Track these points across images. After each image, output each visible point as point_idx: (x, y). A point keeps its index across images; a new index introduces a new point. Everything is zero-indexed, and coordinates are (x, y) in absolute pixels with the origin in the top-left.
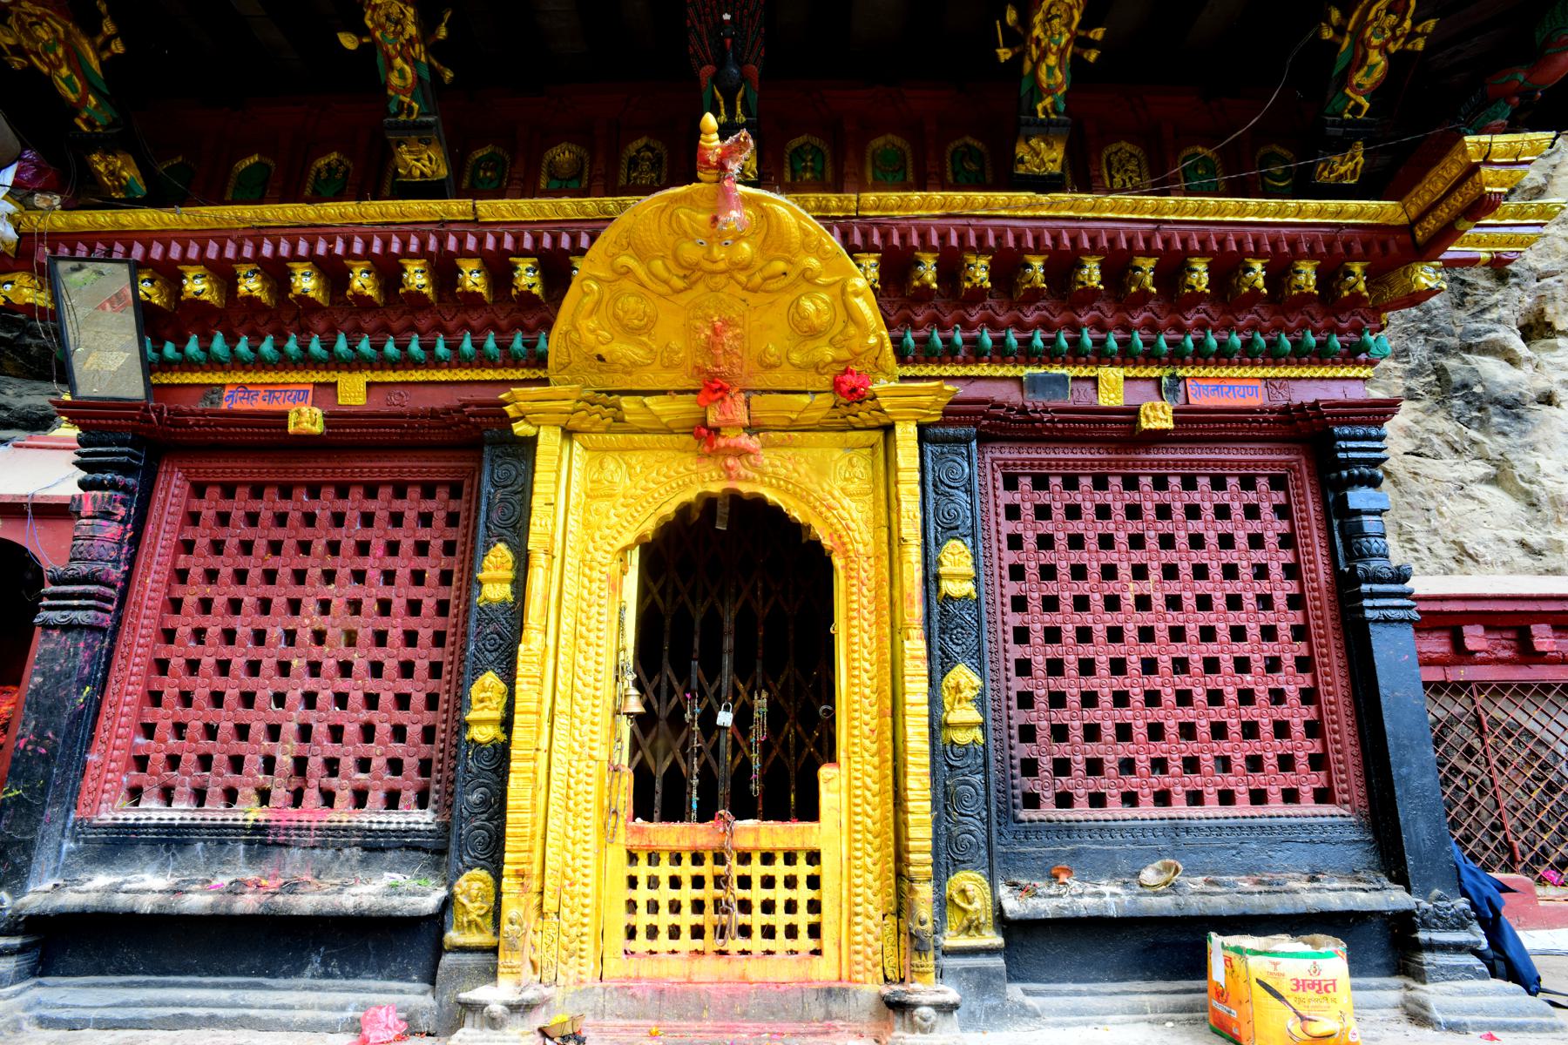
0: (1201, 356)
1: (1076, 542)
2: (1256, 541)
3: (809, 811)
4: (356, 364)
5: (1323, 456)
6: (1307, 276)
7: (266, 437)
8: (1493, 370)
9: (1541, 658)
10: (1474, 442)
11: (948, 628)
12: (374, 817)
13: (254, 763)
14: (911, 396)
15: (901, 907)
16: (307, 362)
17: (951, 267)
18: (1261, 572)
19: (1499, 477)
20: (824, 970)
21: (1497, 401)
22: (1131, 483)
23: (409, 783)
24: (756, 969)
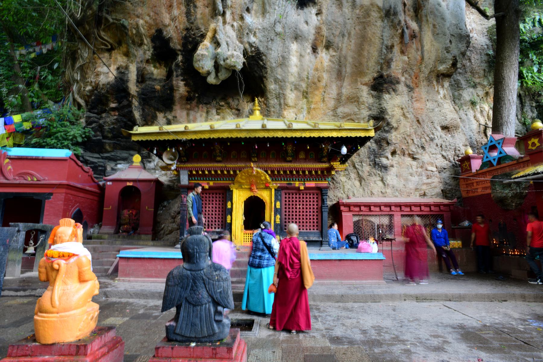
0: (307, 181)
4: (212, 180)
5: (321, 192)
6: (319, 172)
8: (384, 161)
9: (372, 211)
10: (379, 174)
11: (277, 211)
14: (274, 185)
16: (206, 180)
18: (314, 205)
19: (382, 180)
21: (383, 167)
22: (300, 194)
23: (220, 226)
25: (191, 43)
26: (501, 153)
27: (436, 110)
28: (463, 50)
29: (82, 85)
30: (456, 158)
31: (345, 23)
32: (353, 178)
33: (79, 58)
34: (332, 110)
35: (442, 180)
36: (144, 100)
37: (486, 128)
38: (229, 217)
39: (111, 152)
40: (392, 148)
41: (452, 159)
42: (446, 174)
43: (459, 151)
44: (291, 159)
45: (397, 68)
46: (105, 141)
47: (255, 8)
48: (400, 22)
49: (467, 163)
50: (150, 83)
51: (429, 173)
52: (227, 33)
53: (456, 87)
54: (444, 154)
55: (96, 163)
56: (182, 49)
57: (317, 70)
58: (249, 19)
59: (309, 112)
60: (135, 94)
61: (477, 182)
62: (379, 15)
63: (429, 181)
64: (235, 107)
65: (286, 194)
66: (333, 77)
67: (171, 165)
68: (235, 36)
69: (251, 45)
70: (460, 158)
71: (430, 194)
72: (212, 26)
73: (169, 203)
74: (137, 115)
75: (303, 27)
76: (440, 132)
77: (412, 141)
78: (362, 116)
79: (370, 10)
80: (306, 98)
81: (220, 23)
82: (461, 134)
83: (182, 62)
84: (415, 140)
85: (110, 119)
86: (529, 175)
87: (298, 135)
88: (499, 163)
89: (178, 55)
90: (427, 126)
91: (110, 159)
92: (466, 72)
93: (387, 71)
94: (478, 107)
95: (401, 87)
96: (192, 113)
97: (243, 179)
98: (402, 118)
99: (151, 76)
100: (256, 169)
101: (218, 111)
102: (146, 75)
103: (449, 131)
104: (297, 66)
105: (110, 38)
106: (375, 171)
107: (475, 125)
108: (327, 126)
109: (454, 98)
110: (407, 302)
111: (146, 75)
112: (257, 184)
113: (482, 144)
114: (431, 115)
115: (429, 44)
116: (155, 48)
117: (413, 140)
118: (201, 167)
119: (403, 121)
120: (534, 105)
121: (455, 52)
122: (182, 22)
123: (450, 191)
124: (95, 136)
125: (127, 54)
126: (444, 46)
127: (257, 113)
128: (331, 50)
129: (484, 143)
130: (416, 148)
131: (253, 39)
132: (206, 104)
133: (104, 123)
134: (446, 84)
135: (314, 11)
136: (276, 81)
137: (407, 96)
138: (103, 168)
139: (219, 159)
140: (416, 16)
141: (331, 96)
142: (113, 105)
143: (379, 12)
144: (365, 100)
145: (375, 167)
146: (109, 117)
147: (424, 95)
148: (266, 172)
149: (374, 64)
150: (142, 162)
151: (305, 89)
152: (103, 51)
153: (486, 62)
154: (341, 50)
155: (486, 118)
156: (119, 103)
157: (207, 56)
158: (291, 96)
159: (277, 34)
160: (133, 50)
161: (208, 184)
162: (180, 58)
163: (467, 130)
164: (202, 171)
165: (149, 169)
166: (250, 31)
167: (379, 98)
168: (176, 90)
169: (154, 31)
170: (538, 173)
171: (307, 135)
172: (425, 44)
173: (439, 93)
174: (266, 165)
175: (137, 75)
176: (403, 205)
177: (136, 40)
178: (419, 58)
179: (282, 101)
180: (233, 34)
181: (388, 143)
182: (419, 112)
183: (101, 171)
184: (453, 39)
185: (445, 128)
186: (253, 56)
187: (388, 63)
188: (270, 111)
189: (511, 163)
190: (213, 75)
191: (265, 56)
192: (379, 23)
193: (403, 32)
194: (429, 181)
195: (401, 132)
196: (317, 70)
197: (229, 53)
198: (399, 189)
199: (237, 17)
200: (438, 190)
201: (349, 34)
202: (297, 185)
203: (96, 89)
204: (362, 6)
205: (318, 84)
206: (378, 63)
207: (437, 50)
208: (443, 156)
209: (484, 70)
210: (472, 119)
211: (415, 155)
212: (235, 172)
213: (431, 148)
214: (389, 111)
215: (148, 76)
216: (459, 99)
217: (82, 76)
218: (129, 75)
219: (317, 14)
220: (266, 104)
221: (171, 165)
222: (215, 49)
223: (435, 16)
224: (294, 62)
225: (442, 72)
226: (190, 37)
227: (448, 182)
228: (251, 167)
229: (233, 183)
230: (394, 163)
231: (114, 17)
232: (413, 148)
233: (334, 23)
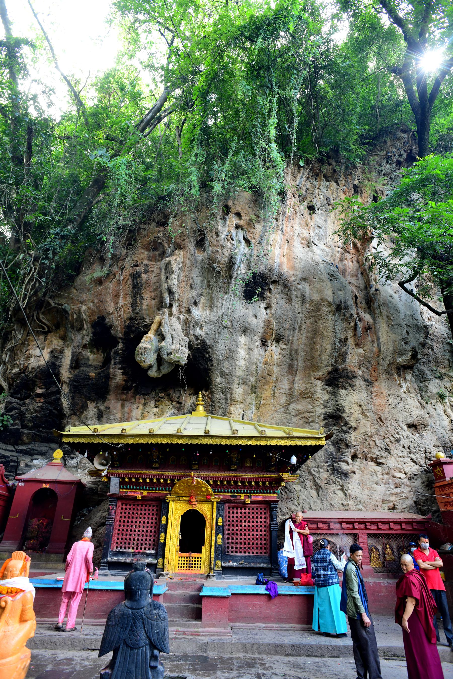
0: (254, 493)
1: (237, 517)
2: (261, 518)
3: (200, 552)
4: (146, 490)
6: (267, 484)
7: (134, 499)
8: (344, 466)
9: (332, 529)
11: (219, 529)
12: (147, 551)
13: (132, 544)
14: (216, 498)
15: (210, 564)
16: (140, 489)
17: (222, 482)
19: (342, 490)
20: (201, 572)
23: (151, 547)
24: (193, 572)
25: (135, 332)
27: (400, 405)
28: (422, 340)
29: (9, 367)
30: (428, 462)
31: (295, 317)
32: (309, 486)
33: (11, 339)
34: (283, 407)
35: (414, 489)
36: (75, 387)
38: (163, 535)
39: (28, 444)
40: (352, 451)
41: (423, 463)
42: (418, 483)
44: (235, 467)
45: (354, 357)
46: (23, 431)
47: (202, 301)
48: (352, 315)
49: (439, 469)
50: (85, 369)
51: (397, 480)
52: (173, 326)
53: (421, 378)
55: (9, 457)
56: (123, 337)
57: (266, 363)
58: (197, 312)
59: (258, 409)
60: (67, 380)
62: (330, 309)
63: (398, 490)
64: (176, 399)
65: (229, 508)
66: (284, 370)
67: (102, 471)
68: (180, 329)
69: (197, 338)
71: (400, 507)
72: (158, 318)
73: (90, 511)
74: (65, 403)
75: (253, 321)
76: (406, 432)
78: (317, 414)
79: (321, 305)
80: (255, 392)
81: (166, 316)
82: (430, 432)
83: (121, 349)
85: (33, 406)
87: (243, 442)
89: (118, 343)
91: (25, 453)
92: (430, 361)
93: (342, 364)
94: (447, 400)
95: (359, 382)
96: (127, 404)
97: (181, 490)
98: (361, 416)
99: (86, 362)
100: (196, 478)
101: (157, 403)
102: (81, 360)
104: (245, 360)
105: (49, 320)
106: (333, 478)
108: (275, 432)
111: (81, 360)
112: (197, 496)
115: (385, 336)
116: (94, 334)
118: (135, 474)
119: (363, 421)
121: (414, 343)
122: (127, 312)
123: (424, 503)
124: (13, 425)
125: (64, 338)
126: (401, 337)
127: (201, 408)
128: (281, 342)
130: (379, 451)
131: (199, 332)
132: (144, 395)
133: (26, 410)
134: (409, 376)
135: (263, 305)
136: (223, 374)
137: (365, 391)
138: (16, 464)
139: (156, 465)
140: (369, 308)
141: (281, 391)
142: (39, 391)
143: (330, 307)
144: (320, 396)
145: (333, 473)
146: (33, 404)
147: (385, 390)
148: (208, 482)
149: (327, 357)
150: (63, 458)
151: (254, 384)
152: (38, 333)
154: (292, 343)
156: (47, 390)
157: (150, 350)
158: (239, 391)
159: (224, 327)
160: (71, 334)
161: (141, 493)
162: (120, 346)
163: (438, 427)
164: (135, 478)
165: (69, 467)
166: (196, 323)
167: (335, 394)
168: (112, 379)
169: (96, 317)
171: (253, 443)
172: (380, 335)
173: (401, 387)
174: (208, 474)
175: (71, 360)
176: (368, 522)
177: (76, 324)
178: (375, 350)
179: (229, 396)
180: (178, 327)
181: (347, 446)
183: (13, 468)
184: (410, 330)
185: (410, 426)
186: (198, 349)
187: (343, 356)
188: (214, 406)
190: (155, 368)
191: (211, 348)
192: (330, 317)
193: (356, 324)
194: (398, 490)
195: (362, 431)
196: (266, 363)
197: (173, 347)
198: (363, 501)
199: (183, 310)
200: (410, 502)
201: (300, 327)
202: (242, 498)
203: (24, 373)
204: (312, 301)
205: (268, 378)
206: (332, 357)
207: (394, 342)
208: (411, 459)
209: (449, 360)
210: (442, 414)
212: (173, 481)
213: (397, 451)
214: (347, 409)
215: (83, 362)
216: (426, 392)
217: (11, 357)
218: (63, 360)
219: (266, 308)
220: (210, 398)
221: (102, 471)
222: (159, 341)
223: (388, 307)
224: (243, 355)
226: (133, 326)
227: (421, 491)
228: (190, 476)
229: (170, 494)
230: (355, 468)
231: (56, 302)
232: (376, 451)
233: (284, 317)
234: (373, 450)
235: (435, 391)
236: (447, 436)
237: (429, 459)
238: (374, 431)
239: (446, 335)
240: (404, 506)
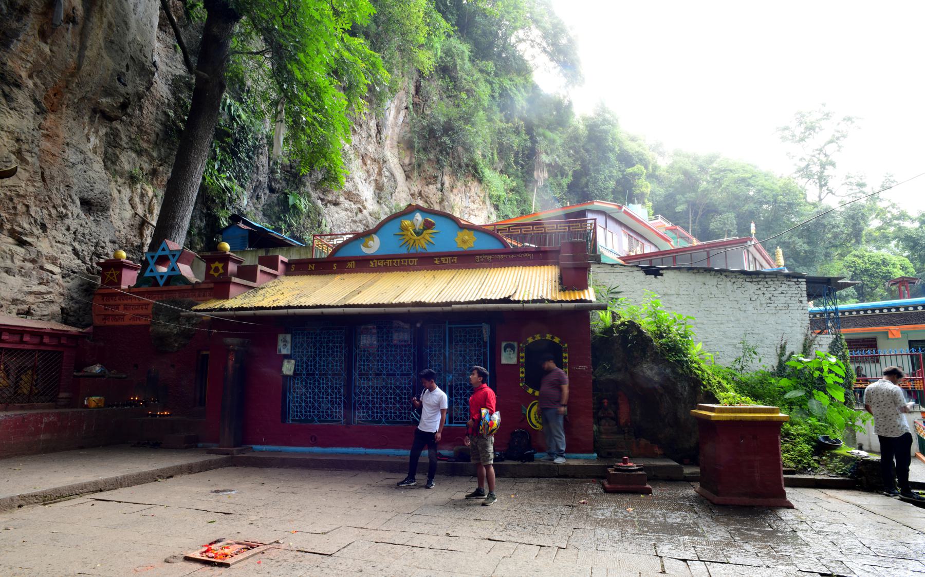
26: (173, 270)
35: (66, 292)
37: (144, 223)
41: (88, 259)
43: (103, 247)
54: (76, 244)
61: (125, 305)
63: (42, 288)
70: (102, 261)
71: (39, 313)
76: (76, 208)
77: (24, 209)
84: (33, 210)
86: (214, 309)
88: (167, 283)
90: (58, 190)
92: (131, 124)
94: (139, 186)
103: (90, 209)
107: (128, 214)
109: (106, 157)
110: (24, 508)
113: (132, 245)
114: (69, 172)
117: (27, 206)
120: (205, 211)
123: (75, 312)
129: (136, 244)
130: (30, 224)
153: (161, 124)
155: (147, 207)
170: (225, 310)
173: (88, 140)
182: (47, 158)
184: (131, 64)
189: (184, 287)
194: (42, 288)
208: (74, 250)
209: (157, 135)
210: (126, 201)
211: (26, 235)
225: (102, 108)
227: (75, 296)
234: (19, 219)
235: (127, 167)
236: (124, 232)
237: (99, 256)
238: (31, 189)
239: (166, 101)
240: (46, 313)
